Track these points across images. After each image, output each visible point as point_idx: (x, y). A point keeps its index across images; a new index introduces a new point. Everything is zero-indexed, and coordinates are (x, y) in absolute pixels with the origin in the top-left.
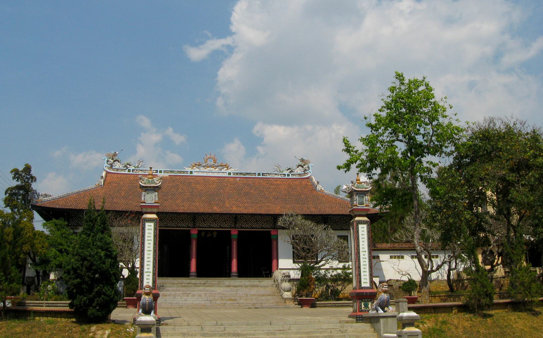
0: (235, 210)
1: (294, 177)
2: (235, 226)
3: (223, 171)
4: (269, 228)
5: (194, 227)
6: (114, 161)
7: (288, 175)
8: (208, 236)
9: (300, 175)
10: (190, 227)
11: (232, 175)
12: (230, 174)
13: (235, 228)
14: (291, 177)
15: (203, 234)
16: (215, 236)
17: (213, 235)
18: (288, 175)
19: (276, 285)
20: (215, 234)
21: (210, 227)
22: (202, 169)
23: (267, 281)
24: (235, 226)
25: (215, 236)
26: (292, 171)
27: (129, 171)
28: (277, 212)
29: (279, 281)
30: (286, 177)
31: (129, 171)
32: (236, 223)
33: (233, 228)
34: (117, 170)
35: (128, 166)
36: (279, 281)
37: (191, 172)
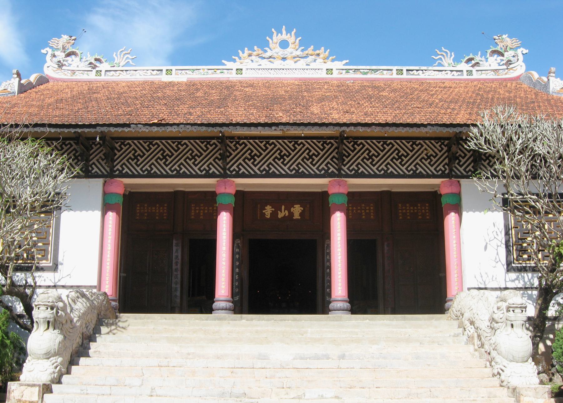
0: (336, 117)
1: (484, 76)
2: (339, 170)
3: (313, 66)
4: (434, 176)
5: (224, 176)
6: (68, 55)
7: (470, 72)
8: (281, 215)
9: (495, 71)
10: (213, 176)
11: (335, 75)
12: (329, 71)
13: (340, 175)
14: (476, 76)
15: (268, 210)
16: (297, 216)
17: (291, 214)
18: (470, 72)
19: (471, 338)
20: (297, 210)
21: (268, 175)
22: (265, 63)
23: (434, 322)
24: (339, 170)
25: (297, 216)
26: (477, 64)
27: (99, 72)
28: (459, 120)
29: (484, 324)
30: (465, 76)
31: (99, 72)
32: (341, 158)
33: (332, 175)
34: (73, 72)
35: (98, 64)
36: (484, 324)
37: (239, 71)
